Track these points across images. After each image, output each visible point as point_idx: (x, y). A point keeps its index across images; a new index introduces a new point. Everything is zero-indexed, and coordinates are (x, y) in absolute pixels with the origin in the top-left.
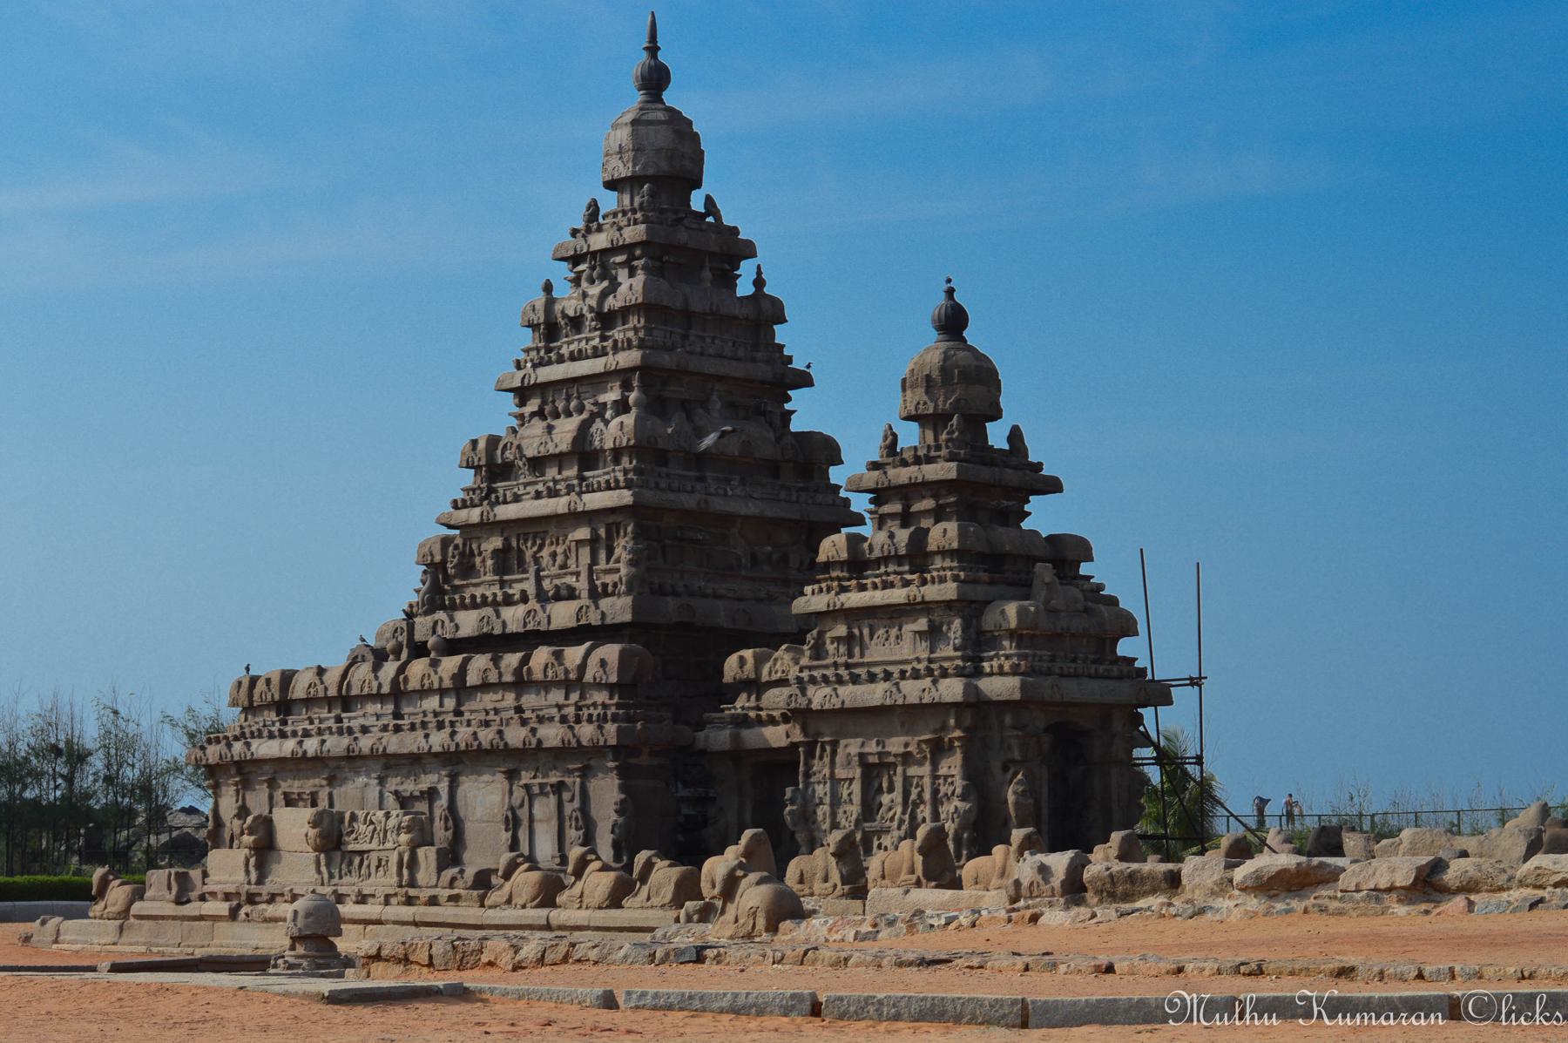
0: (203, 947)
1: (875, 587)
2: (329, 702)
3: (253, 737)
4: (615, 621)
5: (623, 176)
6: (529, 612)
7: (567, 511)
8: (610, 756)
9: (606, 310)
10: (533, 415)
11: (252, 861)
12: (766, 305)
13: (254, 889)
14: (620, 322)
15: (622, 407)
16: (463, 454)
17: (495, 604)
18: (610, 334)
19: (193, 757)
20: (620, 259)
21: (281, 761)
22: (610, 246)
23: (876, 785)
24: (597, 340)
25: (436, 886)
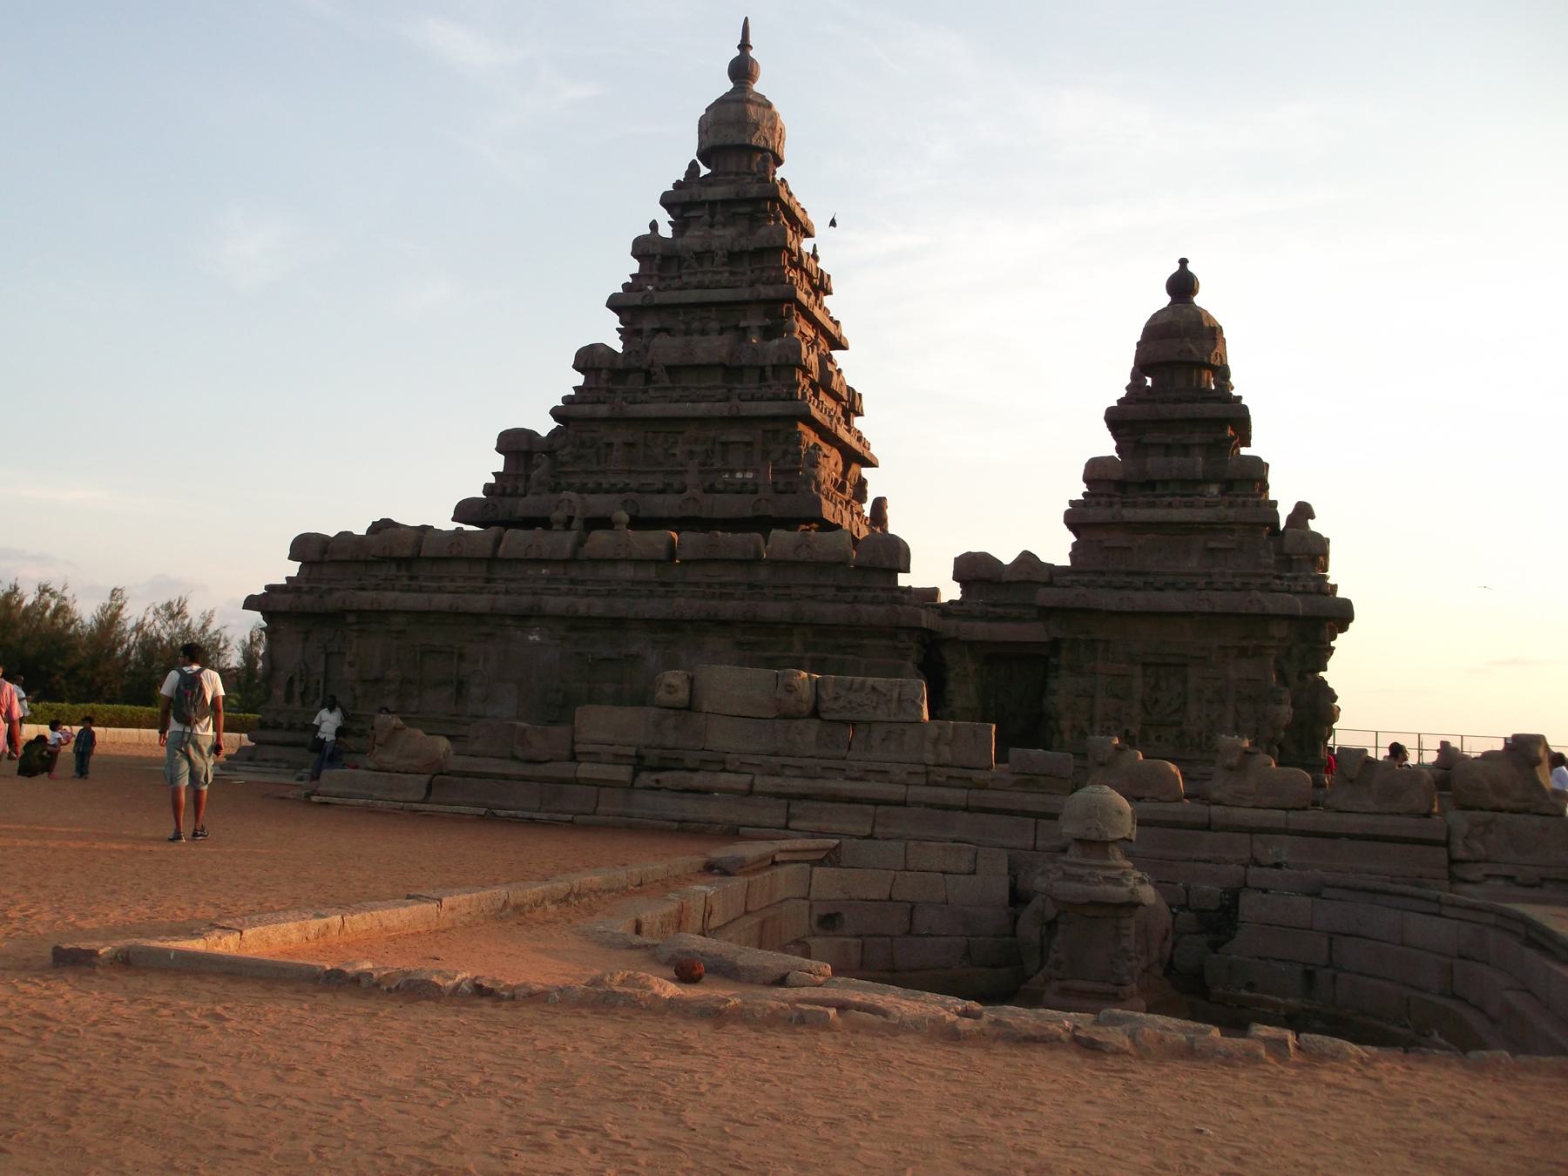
0: (582, 814)
1: (1170, 505)
5: (737, 142)
6: (688, 499)
9: (737, 249)
10: (657, 331)
12: (826, 277)
15: (769, 333)
20: (741, 210)
21: (420, 616)
22: (733, 196)
24: (727, 274)
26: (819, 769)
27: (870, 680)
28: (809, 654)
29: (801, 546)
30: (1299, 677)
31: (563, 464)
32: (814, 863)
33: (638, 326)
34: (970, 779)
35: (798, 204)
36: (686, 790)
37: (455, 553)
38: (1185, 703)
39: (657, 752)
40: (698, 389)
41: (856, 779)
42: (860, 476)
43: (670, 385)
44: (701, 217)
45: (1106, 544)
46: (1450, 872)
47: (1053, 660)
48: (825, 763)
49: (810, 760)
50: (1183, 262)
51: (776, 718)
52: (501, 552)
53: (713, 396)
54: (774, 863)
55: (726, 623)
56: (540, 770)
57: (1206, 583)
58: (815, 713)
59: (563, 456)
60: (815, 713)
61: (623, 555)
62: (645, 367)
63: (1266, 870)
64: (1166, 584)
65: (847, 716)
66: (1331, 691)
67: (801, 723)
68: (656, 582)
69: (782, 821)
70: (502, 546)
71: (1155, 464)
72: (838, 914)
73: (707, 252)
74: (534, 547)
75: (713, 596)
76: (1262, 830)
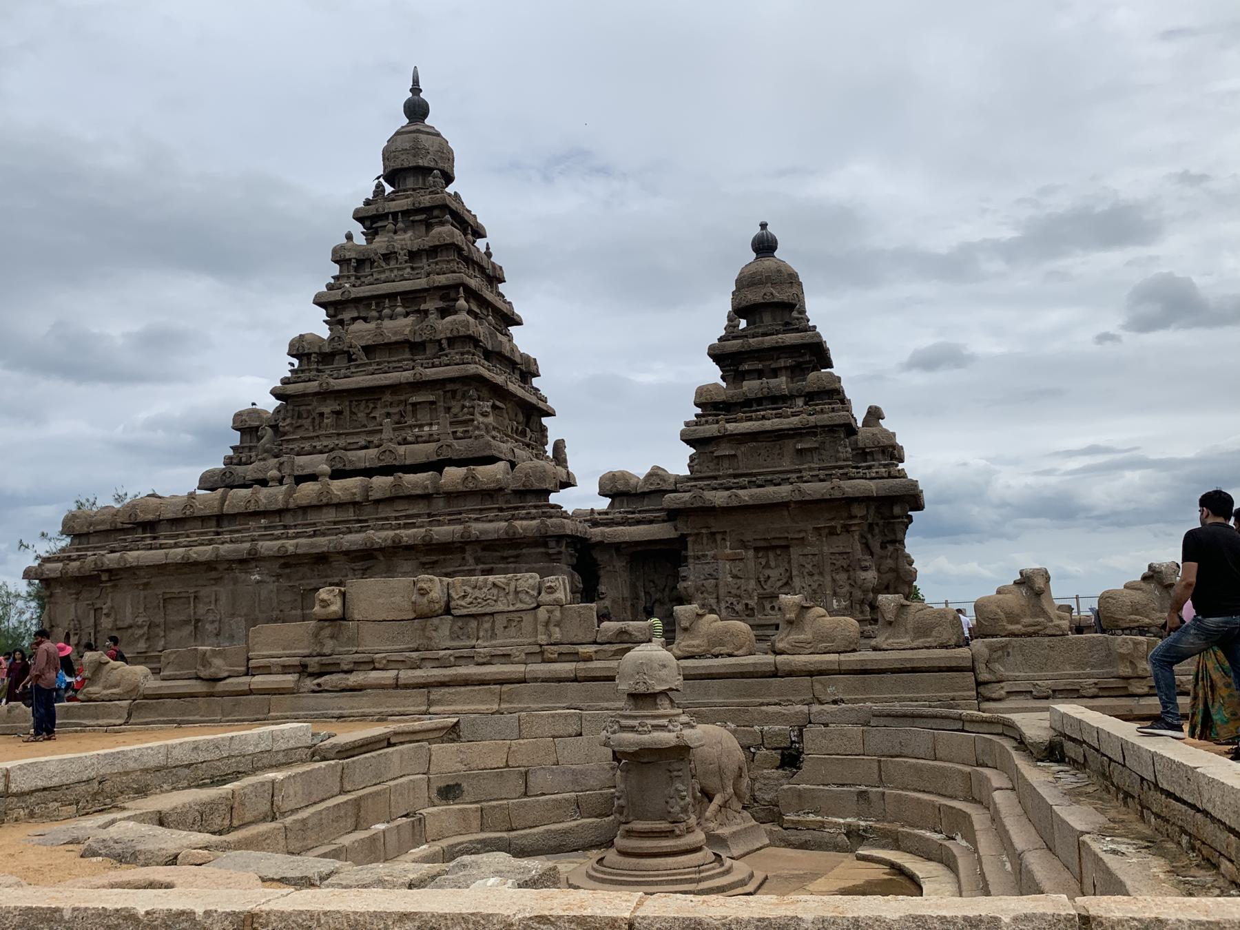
1: (764, 418)
2: (204, 519)
3: (125, 549)
4: (474, 455)
6: (384, 452)
7: (411, 380)
8: (552, 544)
11: (327, 632)
13: (325, 660)
14: (425, 261)
15: (443, 313)
16: (292, 345)
17: (332, 450)
18: (421, 265)
19: (32, 574)
20: (417, 218)
22: (411, 207)
23: (763, 563)
24: (409, 270)
25: (595, 643)
26: (452, 659)
27: (491, 578)
28: (482, 566)
29: (467, 478)
30: (881, 548)
31: (285, 434)
32: (430, 741)
33: (340, 317)
34: (577, 653)
35: (469, 212)
36: (342, 690)
37: (188, 513)
38: (791, 578)
39: (317, 659)
40: (388, 362)
41: (484, 664)
42: (541, 423)
43: (367, 361)
44: (386, 226)
45: (715, 455)
46: (977, 693)
47: (683, 552)
48: (458, 653)
49: (447, 651)
50: (764, 226)
51: (415, 619)
52: (226, 510)
53: (401, 367)
54: (390, 745)
55: (409, 548)
56: (220, 687)
57: (798, 478)
58: (447, 611)
59: (284, 427)
60: (447, 611)
61: (325, 501)
62: (346, 349)
63: (825, 707)
64: (766, 481)
65: (473, 610)
66: (909, 556)
67: (436, 621)
68: (354, 520)
69: (424, 708)
70: (227, 503)
71: (751, 386)
72: (458, 785)
73: (391, 253)
74: (253, 501)
75: (399, 527)
76: (821, 673)
